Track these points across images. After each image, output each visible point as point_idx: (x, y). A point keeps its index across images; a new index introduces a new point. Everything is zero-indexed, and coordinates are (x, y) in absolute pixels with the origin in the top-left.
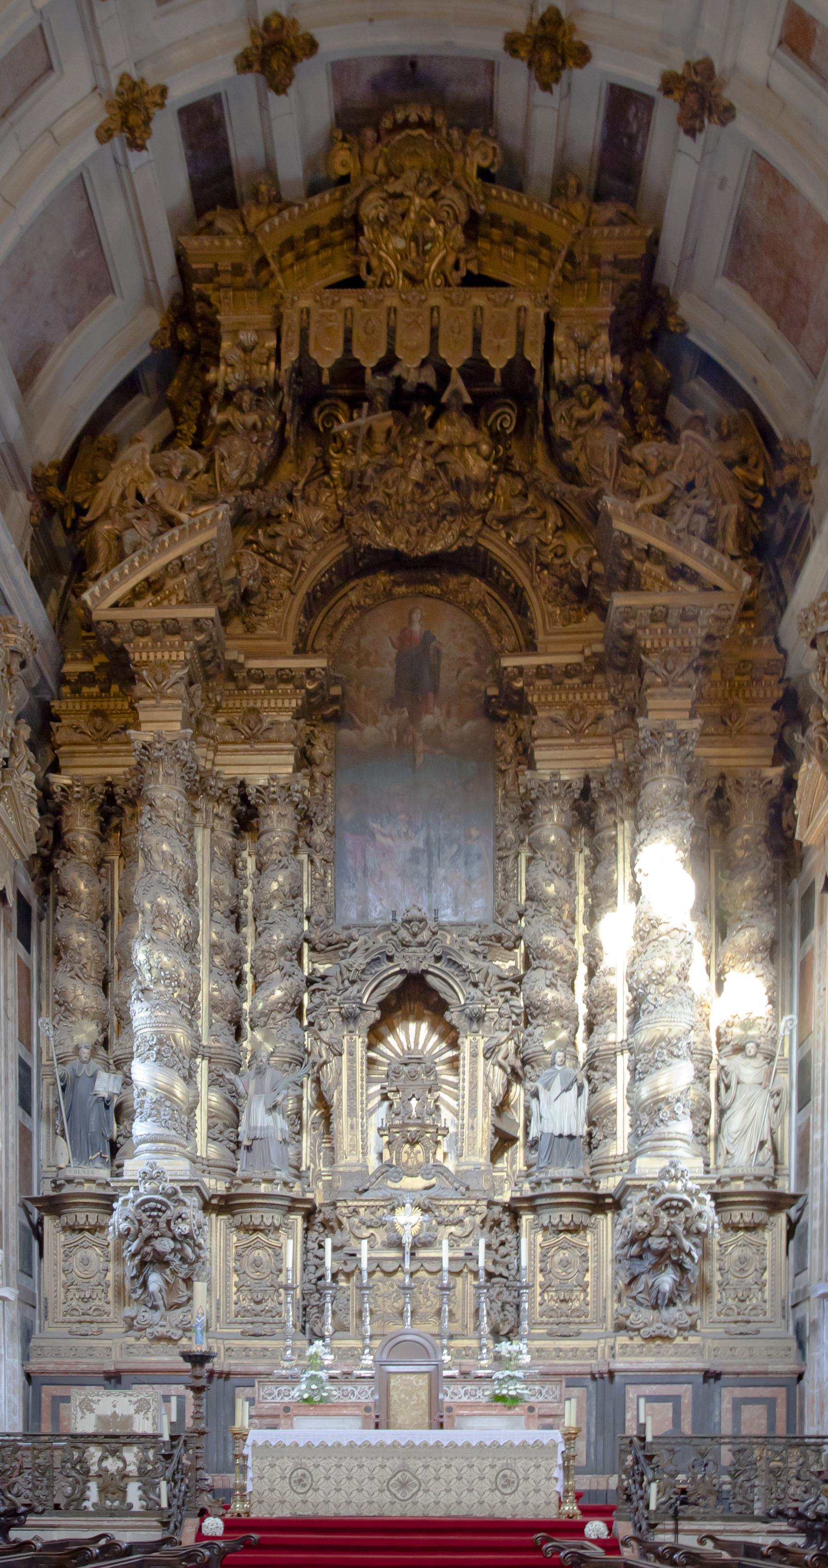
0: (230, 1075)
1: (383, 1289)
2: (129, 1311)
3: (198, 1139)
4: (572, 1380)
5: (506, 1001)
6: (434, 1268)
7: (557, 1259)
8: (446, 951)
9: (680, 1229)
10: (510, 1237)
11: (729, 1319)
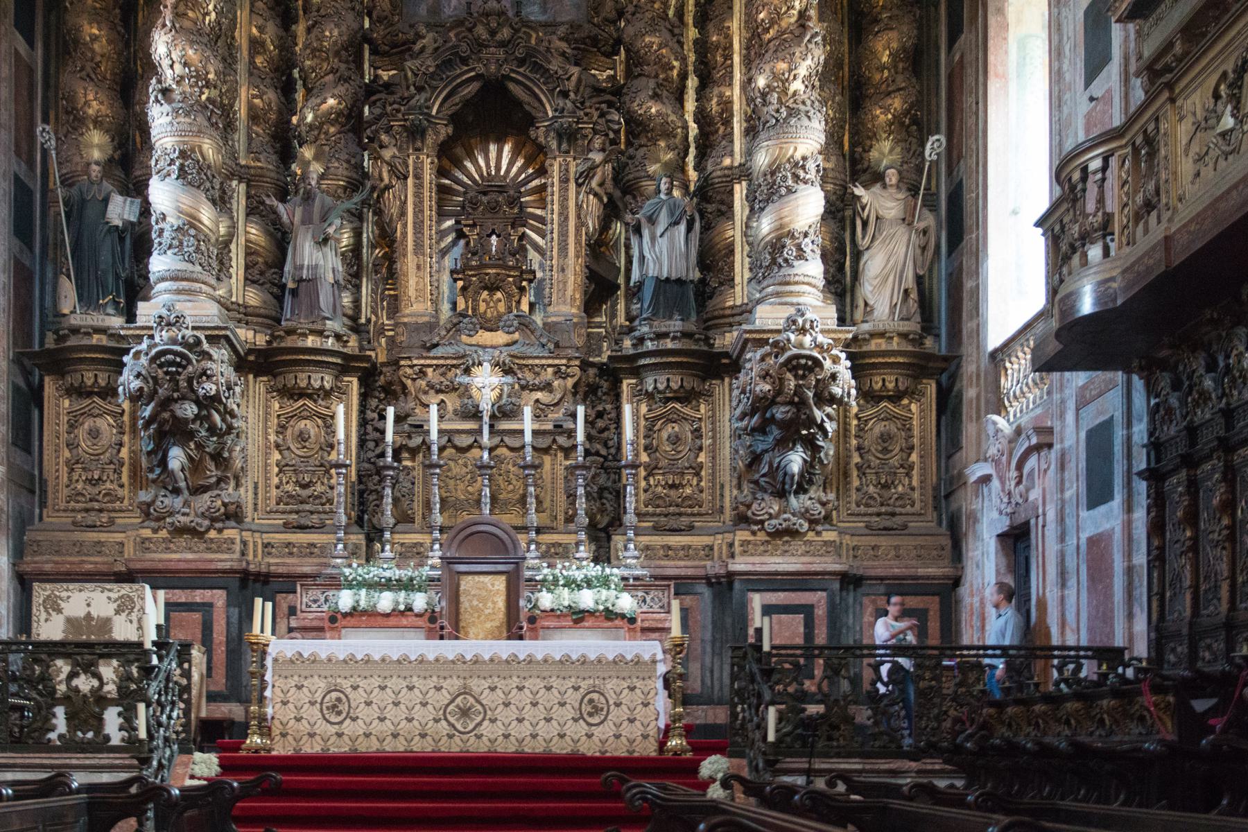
0: (273, 202)
1: (457, 470)
2: (144, 496)
3: (234, 280)
4: (682, 586)
5: (602, 115)
6: (517, 444)
7: (665, 435)
8: (531, 53)
9: (811, 394)
10: (608, 407)
11: (871, 510)
